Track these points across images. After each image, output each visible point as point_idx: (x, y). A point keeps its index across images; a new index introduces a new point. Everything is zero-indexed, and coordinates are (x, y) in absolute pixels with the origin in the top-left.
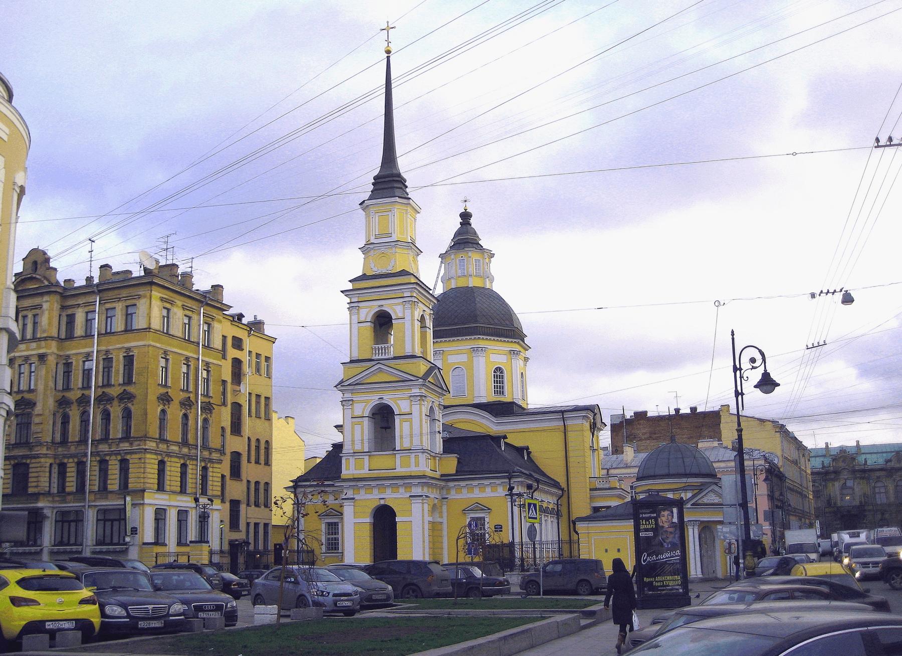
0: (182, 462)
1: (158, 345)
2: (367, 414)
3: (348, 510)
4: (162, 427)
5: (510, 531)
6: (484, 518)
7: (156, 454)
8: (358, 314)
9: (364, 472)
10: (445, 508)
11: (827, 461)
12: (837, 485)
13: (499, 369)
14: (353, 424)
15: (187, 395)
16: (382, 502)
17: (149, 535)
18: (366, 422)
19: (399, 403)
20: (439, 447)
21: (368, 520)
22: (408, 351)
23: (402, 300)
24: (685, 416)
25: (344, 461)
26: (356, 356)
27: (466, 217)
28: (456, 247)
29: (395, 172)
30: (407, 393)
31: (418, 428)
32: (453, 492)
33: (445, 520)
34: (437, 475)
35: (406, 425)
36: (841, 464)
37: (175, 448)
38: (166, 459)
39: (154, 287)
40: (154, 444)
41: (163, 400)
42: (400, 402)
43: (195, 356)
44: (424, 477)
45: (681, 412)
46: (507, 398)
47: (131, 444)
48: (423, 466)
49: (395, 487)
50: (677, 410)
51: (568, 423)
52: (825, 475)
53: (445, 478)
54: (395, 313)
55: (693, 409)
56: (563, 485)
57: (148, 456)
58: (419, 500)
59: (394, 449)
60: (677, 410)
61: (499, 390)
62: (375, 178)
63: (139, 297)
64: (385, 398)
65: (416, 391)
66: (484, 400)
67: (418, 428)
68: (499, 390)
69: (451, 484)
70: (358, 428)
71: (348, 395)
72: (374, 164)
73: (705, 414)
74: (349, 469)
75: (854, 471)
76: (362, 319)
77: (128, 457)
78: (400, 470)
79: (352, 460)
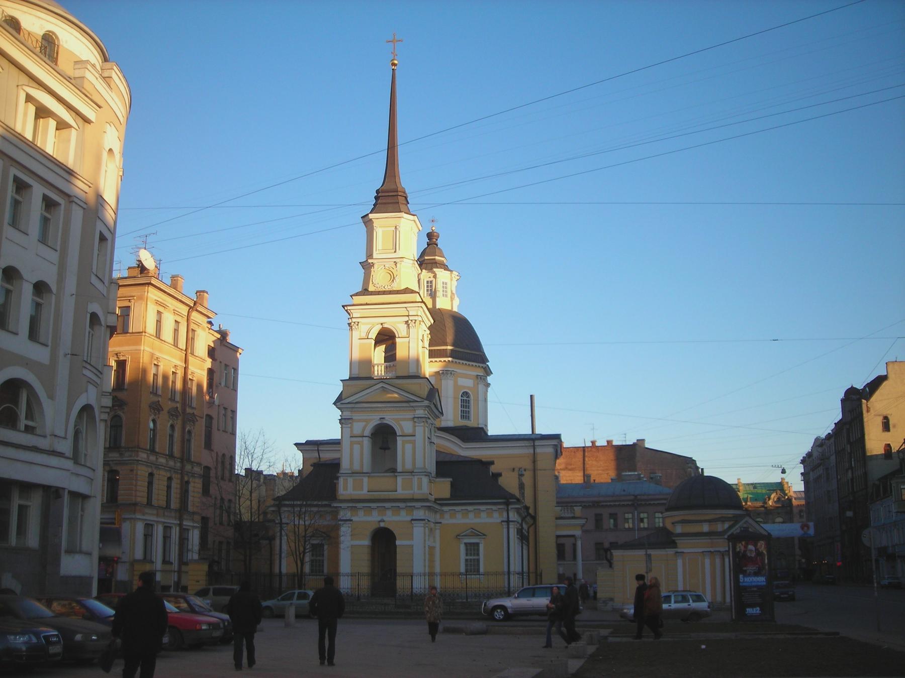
0: (169, 475)
2: (367, 432)
4: (153, 440)
5: (506, 560)
6: (478, 544)
7: (147, 466)
9: (364, 493)
10: (438, 532)
13: (466, 394)
14: (352, 443)
15: (174, 405)
16: (382, 525)
17: (139, 554)
20: (432, 468)
21: (366, 542)
23: (406, 319)
25: (341, 481)
26: (356, 373)
30: (410, 415)
31: (417, 449)
32: (447, 516)
33: (438, 545)
34: (432, 498)
37: (162, 460)
38: (155, 472)
39: (151, 289)
40: (145, 456)
41: (154, 409)
42: (403, 423)
44: (427, 500)
45: (597, 444)
46: (472, 423)
47: (121, 455)
50: (593, 442)
51: (538, 450)
53: (440, 502)
55: (609, 442)
57: (139, 467)
58: (422, 523)
59: (394, 470)
60: (593, 442)
61: (465, 415)
62: (378, 192)
64: (387, 417)
65: (420, 412)
66: (450, 424)
67: (417, 449)
68: (465, 415)
69: (446, 508)
70: (357, 448)
71: (347, 414)
74: (346, 488)
77: (118, 468)
78: (401, 492)
79: (350, 481)
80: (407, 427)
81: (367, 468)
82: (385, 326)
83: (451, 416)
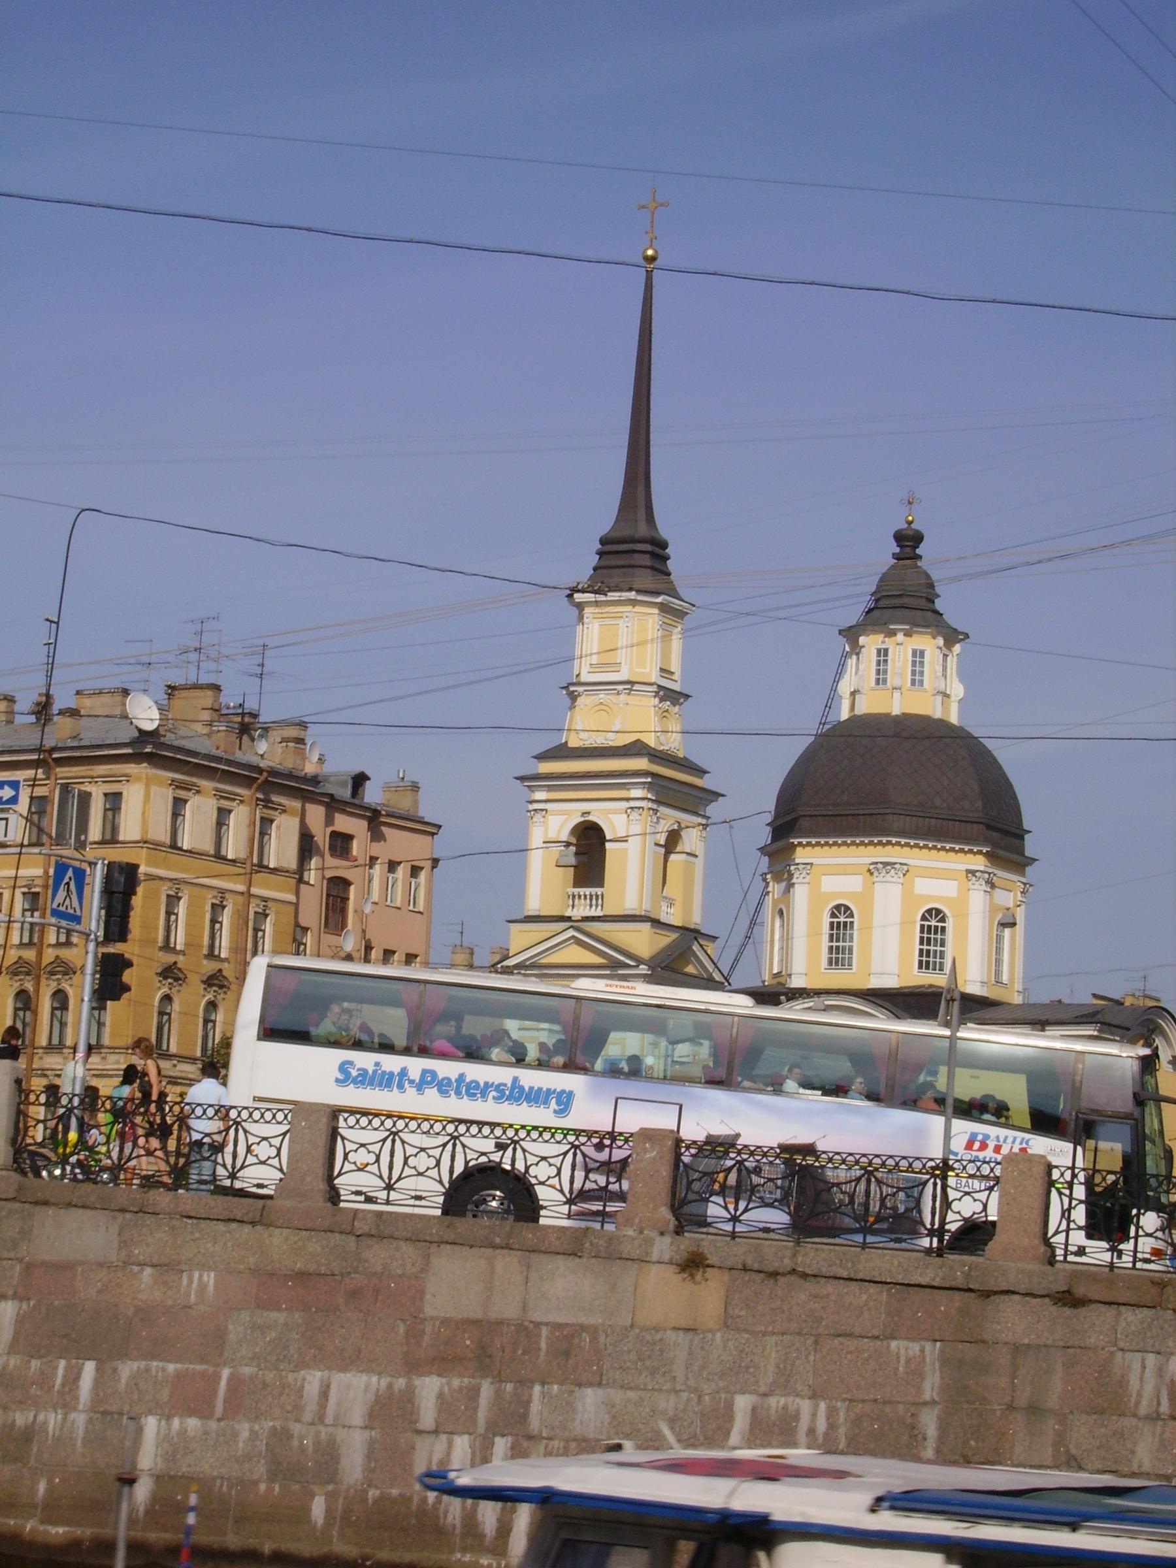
1: (161, 872)
8: (545, 824)
27: (908, 541)
28: (876, 613)
29: (642, 530)
43: (241, 888)
54: (614, 829)
62: (604, 541)
63: (128, 778)
72: (602, 515)
76: (552, 835)
82: (591, 818)
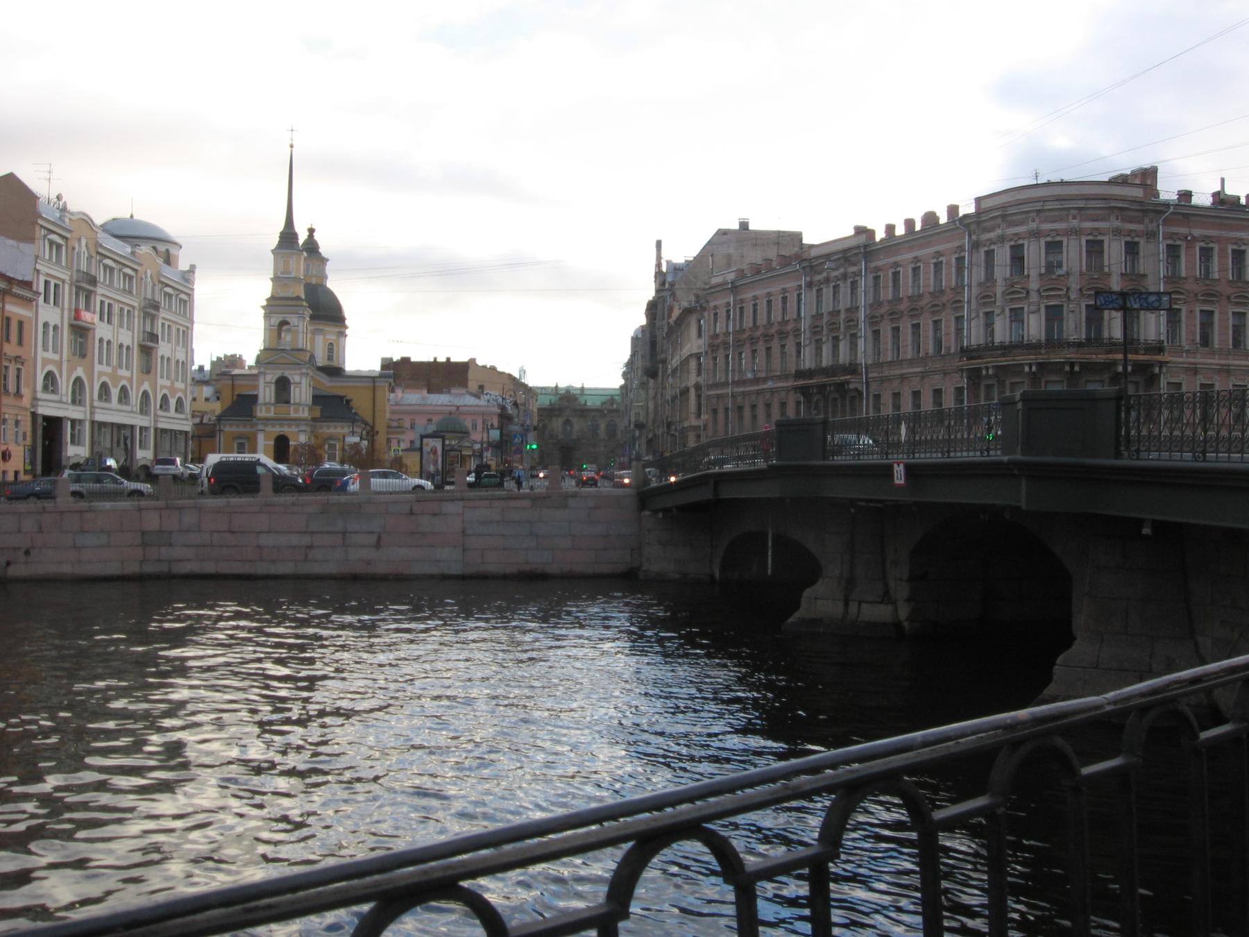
3: (261, 437)
9: (272, 414)
11: (553, 399)
12: (560, 421)
13: (331, 344)
18: (273, 387)
19: (294, 377)
21: (272, 443)
22: (300, 346)
24: (442, 364)
31: (302, 392)
35: (297, 390)
36: (566, 404)
46: (335, 364)
48: (305, 414)
49: (290, 426)
52: (549, 412)
55: (448, 359)
56: (370, 421)
59: (288, 402)
61: (330, 358)
65: (304, 371)
67: (302, 392)
68: (330, 358)
73: (458, 365)
74: (261, 412)
75: (575, 410)
78: (293, 415)
80: (297, 378)
81: (273, 400)
83: (321, 361)
